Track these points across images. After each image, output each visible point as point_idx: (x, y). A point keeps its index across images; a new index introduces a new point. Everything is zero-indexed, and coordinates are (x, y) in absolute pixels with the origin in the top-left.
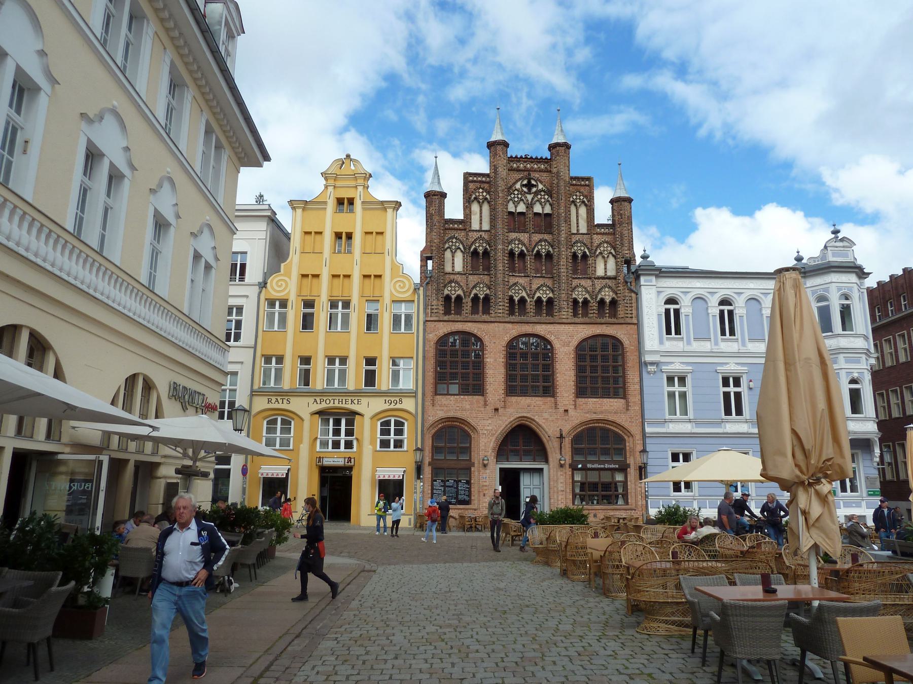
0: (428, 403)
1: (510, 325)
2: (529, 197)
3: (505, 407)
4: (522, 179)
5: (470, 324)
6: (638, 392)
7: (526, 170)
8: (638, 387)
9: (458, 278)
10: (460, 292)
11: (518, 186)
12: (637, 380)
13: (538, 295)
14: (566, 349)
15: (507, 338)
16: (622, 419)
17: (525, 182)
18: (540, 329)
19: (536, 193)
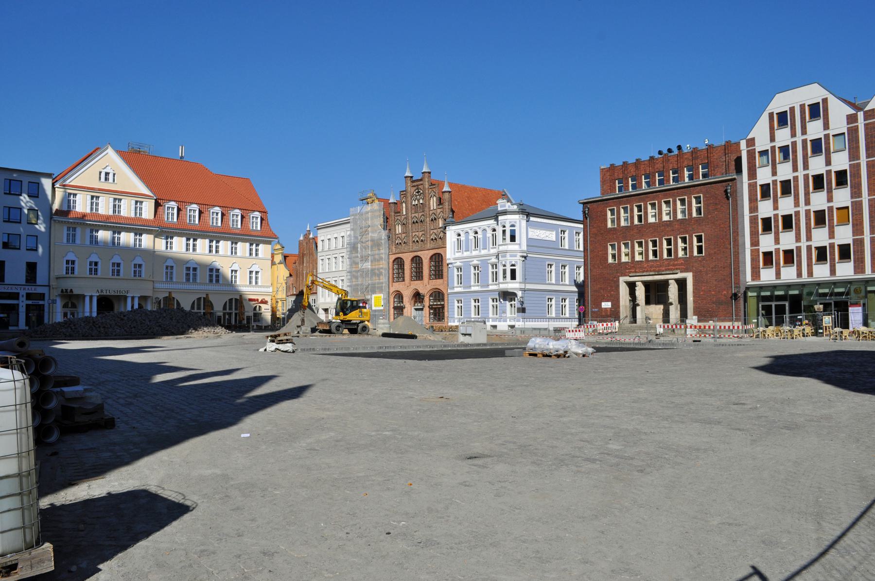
0: (390, 286)
1: (410, 253)
2: (418, 197)
3: (410, 285)
4: (416, 190)
5: (400, 254)
6: (446, 276)
7: (417, 186)
8: (446, 274)
9: (400, 236)
10: (400, 241)
11: (415, 193)
12: (446, 271)
13: (421, 239)
14: (426, 259)
15: (410, 258)
16: (441, 288)
17: (417, 191)
18: (418, 254)
19: (420, 195)
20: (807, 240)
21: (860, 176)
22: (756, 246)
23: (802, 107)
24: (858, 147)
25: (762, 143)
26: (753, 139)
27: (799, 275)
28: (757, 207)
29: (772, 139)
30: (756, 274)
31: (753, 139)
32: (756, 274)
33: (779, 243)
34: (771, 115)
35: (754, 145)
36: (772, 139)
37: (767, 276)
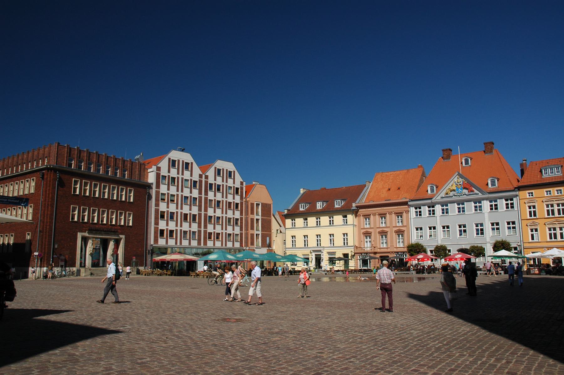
20: (180, 227)
21: (201, 203)
22: (157, 225)
23: (183, 161)
24: (202, 189)
25: (164, 172)
26: (160, 168)
27: (176, 243)
28: (159, 204)
29: (169, 172)
30: (156, 241)
31: (160, 168)
32: (156, 241)
33: (168, 226)
34: (169, 159)
35: (160, 171)
36: (169, 172)
37: (162, 242)
